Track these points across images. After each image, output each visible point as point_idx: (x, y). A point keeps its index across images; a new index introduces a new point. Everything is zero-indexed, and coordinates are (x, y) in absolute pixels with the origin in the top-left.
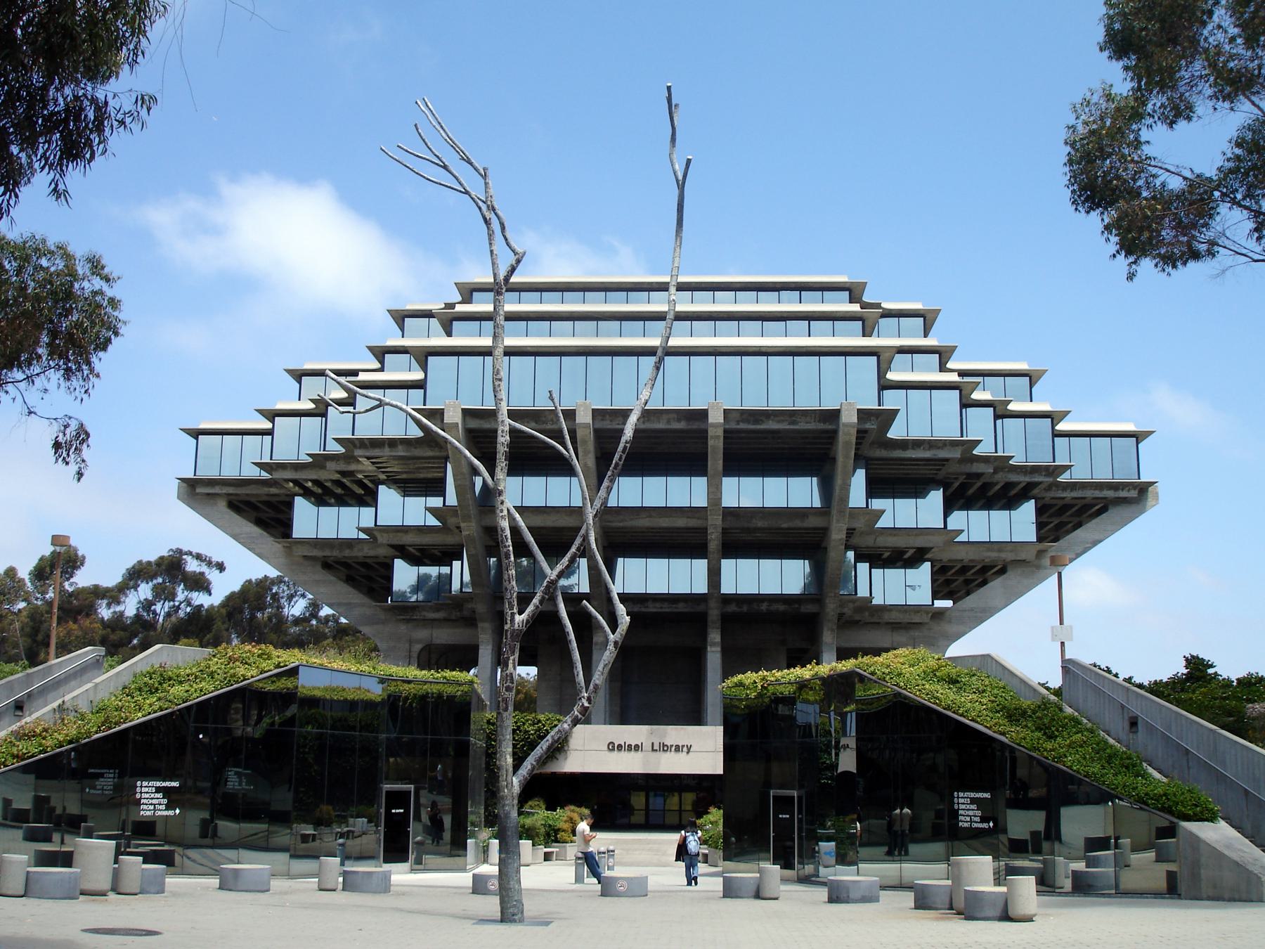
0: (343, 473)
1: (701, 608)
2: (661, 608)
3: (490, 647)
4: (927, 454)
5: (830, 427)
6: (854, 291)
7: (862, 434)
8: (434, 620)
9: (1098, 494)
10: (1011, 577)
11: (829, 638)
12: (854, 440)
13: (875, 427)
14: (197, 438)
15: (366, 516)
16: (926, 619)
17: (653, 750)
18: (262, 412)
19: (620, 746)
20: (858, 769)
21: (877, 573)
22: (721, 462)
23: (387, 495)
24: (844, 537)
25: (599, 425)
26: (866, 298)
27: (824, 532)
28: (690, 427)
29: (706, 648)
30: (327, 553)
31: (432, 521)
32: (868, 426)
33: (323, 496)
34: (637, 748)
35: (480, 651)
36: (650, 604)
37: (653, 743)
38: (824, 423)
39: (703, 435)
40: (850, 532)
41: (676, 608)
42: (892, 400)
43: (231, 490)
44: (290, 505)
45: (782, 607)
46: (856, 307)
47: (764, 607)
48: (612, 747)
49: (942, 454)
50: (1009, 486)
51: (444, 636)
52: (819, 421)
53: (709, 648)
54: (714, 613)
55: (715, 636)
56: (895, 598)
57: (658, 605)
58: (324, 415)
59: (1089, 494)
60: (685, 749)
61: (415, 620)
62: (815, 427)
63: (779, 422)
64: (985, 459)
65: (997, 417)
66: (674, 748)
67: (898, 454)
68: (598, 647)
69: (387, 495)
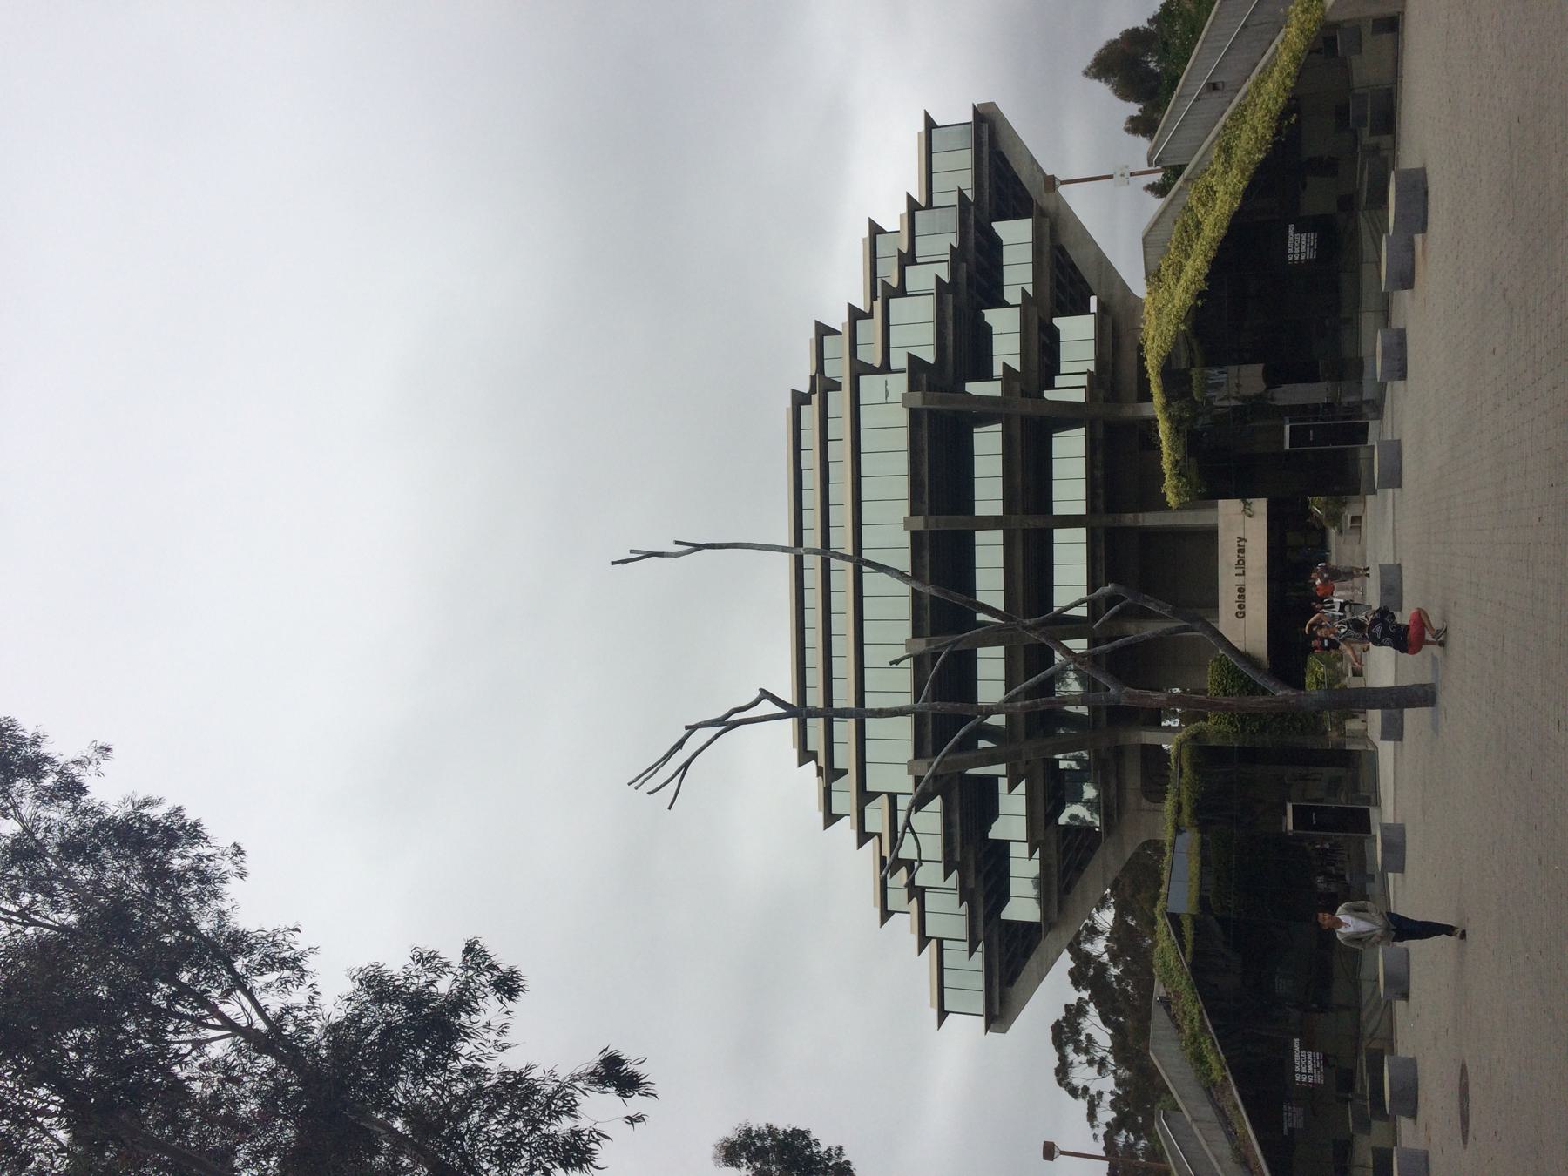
0: (978, 871)
2: (1101, 570)
3: (1143, 733)
4: (950, 325)
6: (799, 400)
7: (931, 387)
8: (1118, 787)
9: (986, 162)
10: (1067, 240)
11: (1129, 411)
12: (937, 394)
13: (925, 375)
14: (948, 1013)
15: (1019, 851)
16: (1109, 320)
17: (1244, 574)
18: (921, 949)
19: (1239, 606)
21: (1064, 368)
22: (961, 517)
23: (997, 832)
24: (1029, 400)
25: (928, 631)
26: (805, 388)
27: (1025, 419)
28: (928, 547)
29: (1140, 527)
30: (1055, 888)
31: (1021, 788)
32: (924, 381)
33: (1003, 896)
34: (1241, 589)
35: (1147, 742)
39: (935, 535)
40: (1024, 394)
42: (899, 360)
43: (996, 980)
44: (1010, 924)
45: (1099, 457)
46: (815, 398)
47: (1099, 474)
48: (1241, 614)
49: (950, 311)
50: (977, 244)
51: (1133, 780)
53: (1141, 524)
54: (1107, 520)
55: (1128, 519)
56: (1089, 351)
58: (923, 890)
59: (986, 171)
60: (1242, 543)
61: (1118, 805)
64: (954, 271)
65: (913, 262)
66: (1241, 555)
67: (950, 350)
69: (997, 832)
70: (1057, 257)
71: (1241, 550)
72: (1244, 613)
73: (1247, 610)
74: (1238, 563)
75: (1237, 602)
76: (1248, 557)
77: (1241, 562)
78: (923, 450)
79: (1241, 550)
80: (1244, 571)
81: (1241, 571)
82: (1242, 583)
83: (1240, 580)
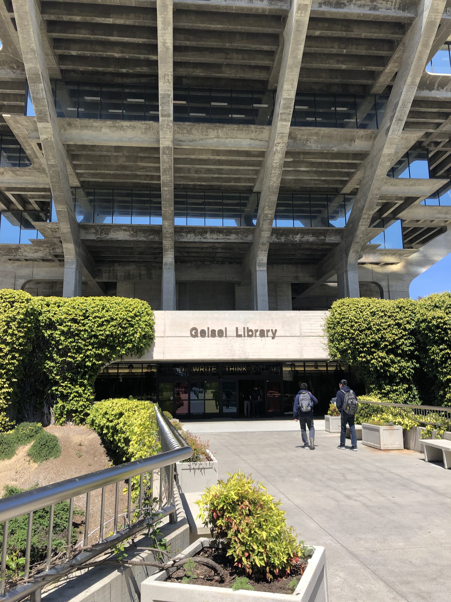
1: (250, 238)
2: (217, 239)
5: (409, 15)
17: (238, 336)
28: (272, 7)
34: (221, 333)
36: (208, 235)
37: (237, 328)
38: (404, 10)
41: (229, 239)
53: (257, 269)
57: (215, 236)
62: (395, 14)
66: (258, 334)
68: (167, 267)
71: (263, 334)
72: (196, 336)
73: (199, 339)
74: (249, 330)
75: (208, 329)
76: (257, 341)
77: (250, 333)
79: (263, 334)
80: (240, 336)
81: (241, 332)
82: (228, 334)
83: (231, 332)
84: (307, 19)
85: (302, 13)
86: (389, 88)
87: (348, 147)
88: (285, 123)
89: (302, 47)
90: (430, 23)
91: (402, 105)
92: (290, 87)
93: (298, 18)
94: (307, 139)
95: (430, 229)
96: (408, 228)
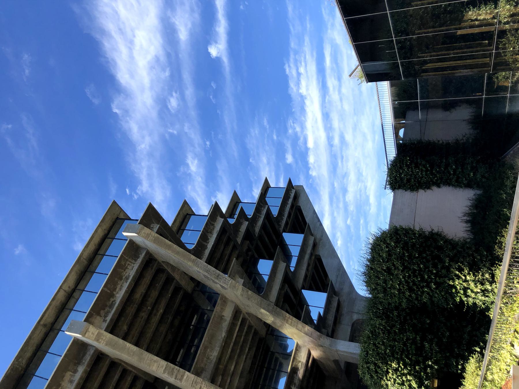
5: (143, 254)
16: (336, 299)
20: (403, 137)
28: (86, 363)
38: (138, 257)
52: (136, 260)
62: (138, 264)
63: (120, 289)
70: (316, 264)
78: (127, 278)
84: (109, 335)
85: (102, 339)
86: (192, 279)
87: (226, 322)
88: (185, 377)
89: (128, 345)
90: (155, 241)
91: (207, 272)
92: (156, 364)
93: (105, 343)
94: (207, 358)
95: (316, 267)
96: (311, 284)
